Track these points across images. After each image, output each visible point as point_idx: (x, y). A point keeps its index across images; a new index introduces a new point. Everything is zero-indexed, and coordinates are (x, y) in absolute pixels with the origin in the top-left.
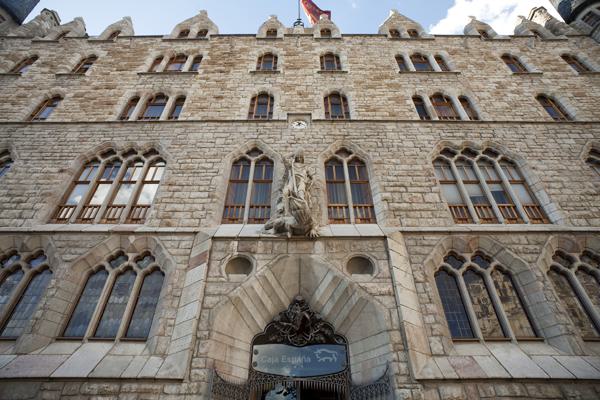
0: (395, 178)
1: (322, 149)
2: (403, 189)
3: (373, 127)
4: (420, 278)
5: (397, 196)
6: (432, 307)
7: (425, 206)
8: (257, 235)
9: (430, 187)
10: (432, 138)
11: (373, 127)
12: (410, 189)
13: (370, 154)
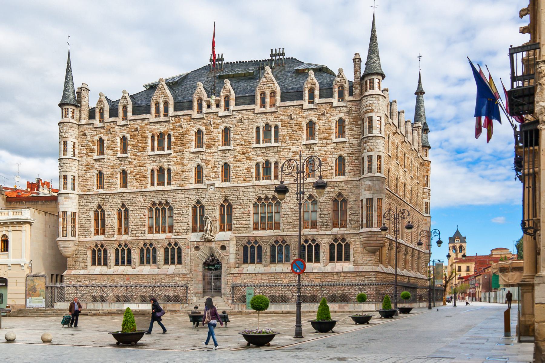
0: (238, 215)
1: (218, 202)
2: (240, 219)
3: (236, 189)
4: (237, 250)
5: (238, 222)
6: (238, 257)
7: (245, 226)
8: (200, 240)
9: (248, 218)
10: (254, 195)
11: (236, 189)
12: (243, 219)
13: (233, 204)
